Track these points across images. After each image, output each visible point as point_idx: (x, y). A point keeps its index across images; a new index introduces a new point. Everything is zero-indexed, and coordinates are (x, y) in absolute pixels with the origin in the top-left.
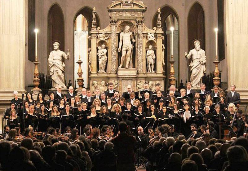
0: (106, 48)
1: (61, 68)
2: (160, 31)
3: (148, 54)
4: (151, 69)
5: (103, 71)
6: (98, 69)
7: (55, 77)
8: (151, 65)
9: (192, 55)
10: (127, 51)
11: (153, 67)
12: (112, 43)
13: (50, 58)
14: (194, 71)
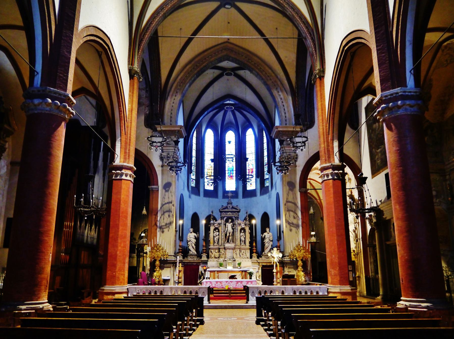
0: (219, 231)
1: (194, 242)
2: (248, 222)
3: (241, 235)
4: (243, 244)
5: (217, 244)
6: (214, 242)
7: (190, 248)
8: (243, 241)
9: (265, 236)
10: (229, 233)
11: (243, 242)
12: (221, 228)
13: (188, 238)
14: (266, 245)
